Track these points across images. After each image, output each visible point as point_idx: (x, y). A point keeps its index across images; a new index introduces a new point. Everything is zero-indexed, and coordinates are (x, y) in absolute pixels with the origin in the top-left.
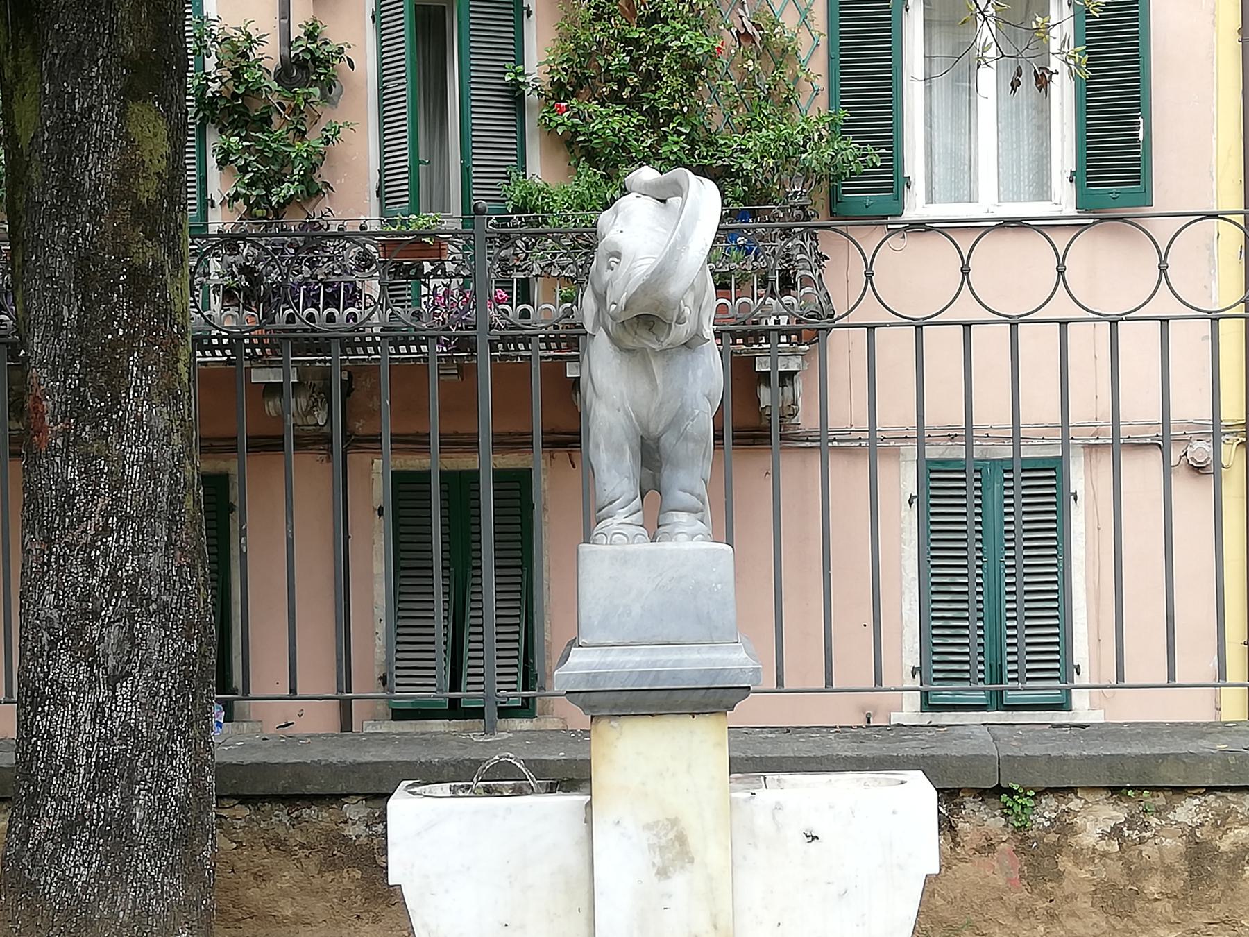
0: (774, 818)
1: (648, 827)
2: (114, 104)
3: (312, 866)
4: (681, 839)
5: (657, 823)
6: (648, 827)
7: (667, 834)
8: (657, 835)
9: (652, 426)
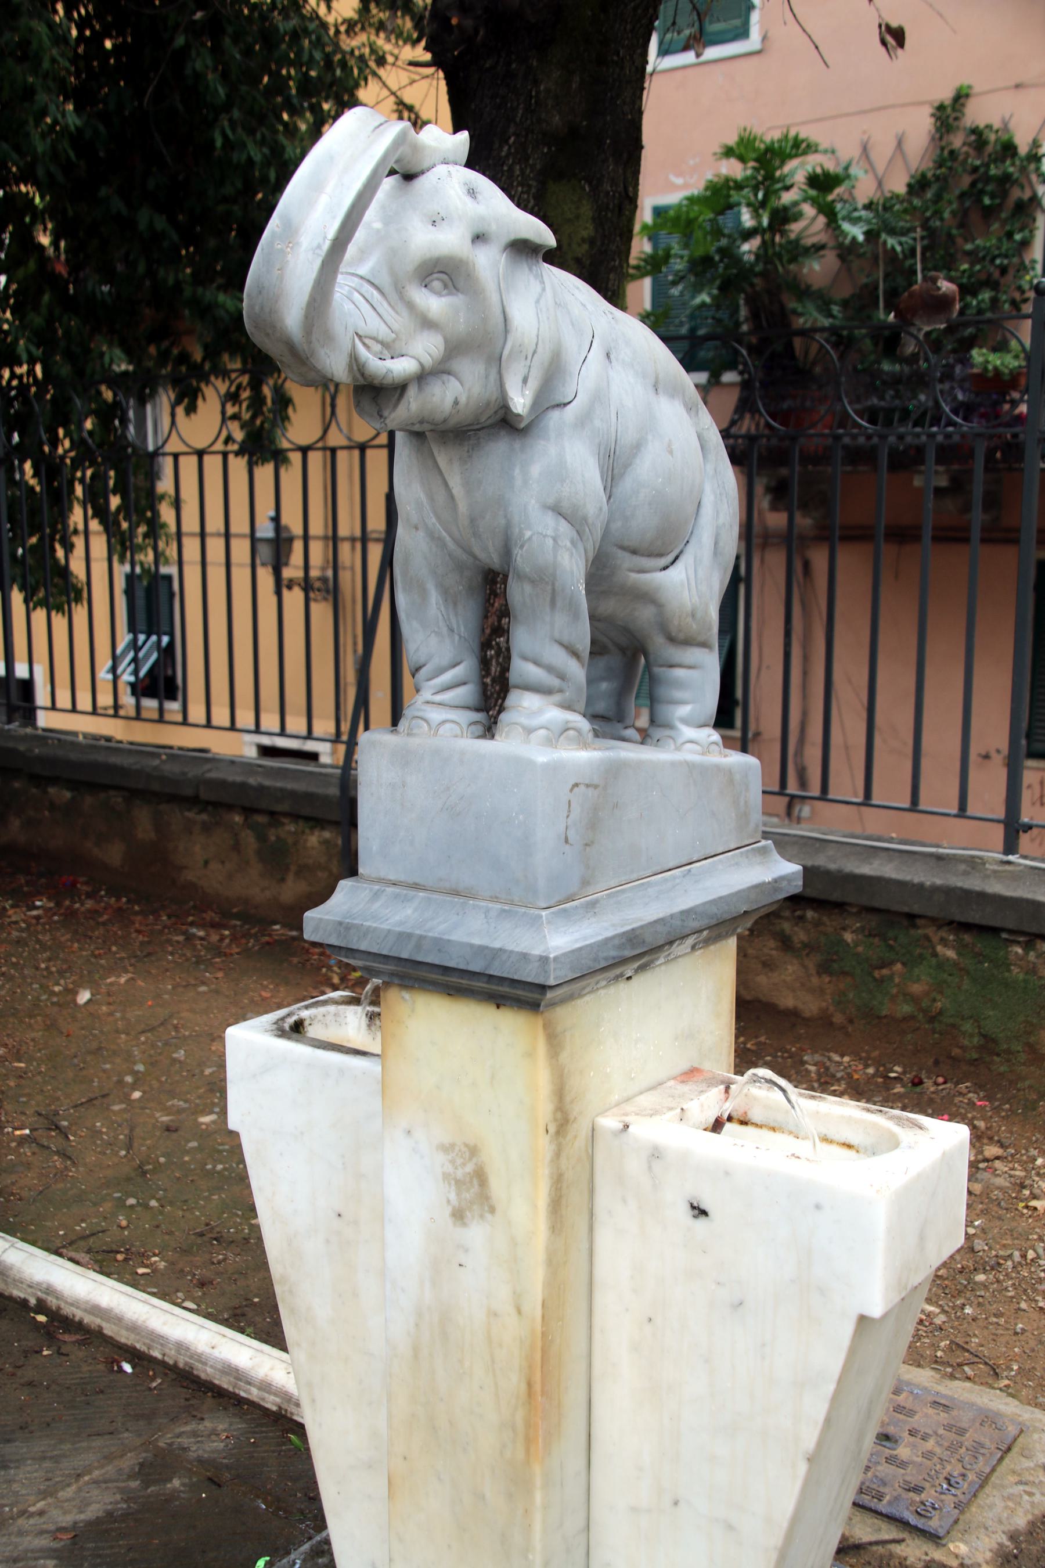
0: (650, 1168)
1: (446, 1148)
2: (529, 186)
3: (811, 964)
4: (480, 1177)
5: (452, 1146)
6: (446, 1148)
7: (464, 1164)
8: (453, 1162)
9: (482, 555)
